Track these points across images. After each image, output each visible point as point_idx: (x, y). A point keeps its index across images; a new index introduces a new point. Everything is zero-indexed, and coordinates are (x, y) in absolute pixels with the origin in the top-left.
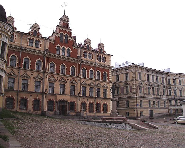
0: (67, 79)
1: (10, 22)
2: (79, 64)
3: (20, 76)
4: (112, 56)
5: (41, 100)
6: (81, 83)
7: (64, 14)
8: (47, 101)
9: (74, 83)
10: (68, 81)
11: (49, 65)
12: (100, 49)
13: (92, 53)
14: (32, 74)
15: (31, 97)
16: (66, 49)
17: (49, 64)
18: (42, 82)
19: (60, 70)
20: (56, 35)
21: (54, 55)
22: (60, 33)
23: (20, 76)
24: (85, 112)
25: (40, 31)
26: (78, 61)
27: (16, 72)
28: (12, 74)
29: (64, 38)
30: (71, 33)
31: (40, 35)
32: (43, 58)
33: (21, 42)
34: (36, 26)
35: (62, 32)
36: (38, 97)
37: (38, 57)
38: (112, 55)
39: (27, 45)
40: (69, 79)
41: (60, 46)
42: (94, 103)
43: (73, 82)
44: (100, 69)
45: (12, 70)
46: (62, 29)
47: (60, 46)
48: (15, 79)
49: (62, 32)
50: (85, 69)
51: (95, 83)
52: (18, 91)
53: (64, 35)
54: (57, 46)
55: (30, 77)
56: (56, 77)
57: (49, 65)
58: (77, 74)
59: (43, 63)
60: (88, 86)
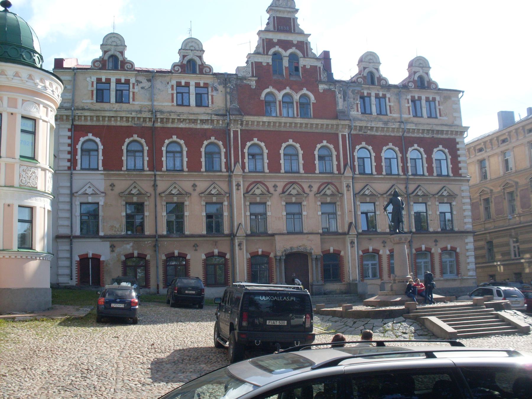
0: (305, 186)
1: (113, 48)
2: (344, 136)
4: (463, 92)
5: (228, 256)
6: (357, 191)
8: (249, 256)
9: (333, 195)
10: (311, 191)
11: (246, 150)
12: (416, 78)
13: (388, 95)
14: (194, 186)
15: (196, 250)
18: (226, 203)
19: (282, 161)
20: (260, 60)
23: (159, 194)
25: (207, 59)
27: (146, 186)
28: (133, 192)
29: (286, 63)
30: (307, 44)
31: (208, 70)
33: (151, 99)
35: (277, 48)
36: (217, 248)
37: (205, 134)
38: (460, 92)
40: (312, 185)
41: (275, 92)
43: (329, 192)
44: (421, 142)
45: (135, 182)
48: (145, 204)
49: (277, 48)
51: (406, 188)
52: (156, 237)
55: (188, 194)
56: (270, 185)
57: (243, 154)
58: (338, 166)
59: (225, 146)
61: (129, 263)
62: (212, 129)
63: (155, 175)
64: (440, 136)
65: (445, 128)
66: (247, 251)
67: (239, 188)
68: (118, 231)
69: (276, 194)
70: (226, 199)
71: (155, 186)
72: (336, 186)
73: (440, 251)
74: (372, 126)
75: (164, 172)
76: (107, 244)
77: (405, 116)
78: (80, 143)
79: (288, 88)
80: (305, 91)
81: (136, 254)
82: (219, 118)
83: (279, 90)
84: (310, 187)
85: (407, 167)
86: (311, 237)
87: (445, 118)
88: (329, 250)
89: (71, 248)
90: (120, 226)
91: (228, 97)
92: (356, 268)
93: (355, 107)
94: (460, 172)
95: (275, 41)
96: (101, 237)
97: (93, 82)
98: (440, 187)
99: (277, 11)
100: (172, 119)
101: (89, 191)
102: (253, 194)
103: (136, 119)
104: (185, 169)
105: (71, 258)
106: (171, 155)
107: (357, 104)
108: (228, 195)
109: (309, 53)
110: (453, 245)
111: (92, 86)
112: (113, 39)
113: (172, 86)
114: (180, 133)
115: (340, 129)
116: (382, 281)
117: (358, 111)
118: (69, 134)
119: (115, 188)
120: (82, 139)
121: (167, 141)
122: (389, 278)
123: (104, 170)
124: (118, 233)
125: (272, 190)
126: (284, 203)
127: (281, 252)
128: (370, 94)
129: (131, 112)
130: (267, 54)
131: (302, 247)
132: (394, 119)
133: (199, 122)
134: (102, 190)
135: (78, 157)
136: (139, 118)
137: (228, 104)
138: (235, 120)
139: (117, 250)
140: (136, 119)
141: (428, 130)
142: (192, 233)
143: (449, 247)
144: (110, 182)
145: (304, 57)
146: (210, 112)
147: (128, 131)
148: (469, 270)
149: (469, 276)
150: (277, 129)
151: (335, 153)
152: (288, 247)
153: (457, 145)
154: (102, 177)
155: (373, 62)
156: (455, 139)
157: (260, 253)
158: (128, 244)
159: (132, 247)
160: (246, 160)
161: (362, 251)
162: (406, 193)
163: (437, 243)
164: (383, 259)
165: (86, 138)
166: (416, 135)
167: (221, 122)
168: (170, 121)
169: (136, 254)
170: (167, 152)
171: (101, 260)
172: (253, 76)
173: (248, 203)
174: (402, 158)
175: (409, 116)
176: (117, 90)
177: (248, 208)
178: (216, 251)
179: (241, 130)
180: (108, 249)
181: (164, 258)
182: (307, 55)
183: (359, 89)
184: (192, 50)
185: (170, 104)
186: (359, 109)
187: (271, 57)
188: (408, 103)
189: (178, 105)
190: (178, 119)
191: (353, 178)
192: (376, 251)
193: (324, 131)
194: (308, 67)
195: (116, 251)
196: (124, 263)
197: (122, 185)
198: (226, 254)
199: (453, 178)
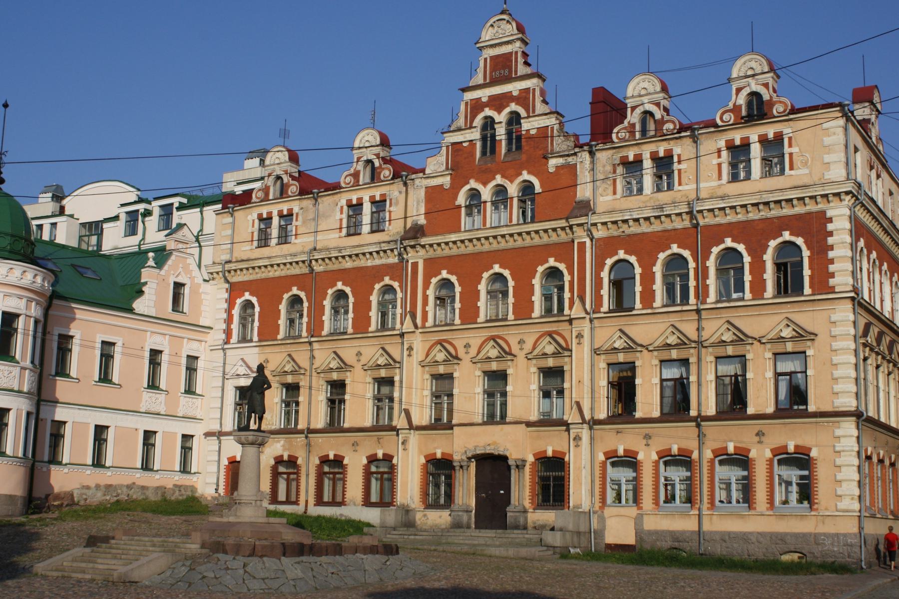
3: (314, 370)
9: (556, 354)
10: (521, 349)
13: (677, 151)
14: (359, 354)
15: (355, 451)
16: (513, 189)
17: (426, 286)
18: (397, 378)
21: (453, 237)
24: (633, 511)
26: (571, 227)
29: (501, 132)
34: (366, 138)
35: (488, 112)
37: (377, 273)
39: (337, 235)
41: (479, 187)
42: (695, 455)
43: (550, 349)
46: (484, 94)
47: (479, 187)
49: (488, 112)
50: (628, 261)
51: (698, 329)
53: (501, 118)
54: (467, 187)
56: (459, 345)
59: (402, 291)
60: (645, 351)
63: (310, 343)
64: (787, 211)
66: (420, 452)
67: (412, 352)
68: (269, 424)
71: (313, 357)
73: (768, 454)
74: (635, 217)
75: (325, 336)
79: (498, 177)
83: (485, 184)
84: (521, 342)
85: (706, 287)
90: (272, 417)
92: (581, 484)
94: (832, 282)
95: (484, 100)
97: (253, 221)
104: (350, 330)
110: (800, 443)
111: (253, 226)
113: (342, 207)
118: (226, 295)
120: (239, 301)
121: (330, 292)
122: (654, 506)
123: (260, 341)
124: (269, 427)
127: (460, 454)
129: (285, 256)
130: (471, 127)
131: (492, 447)
135: (235, 326)
141: (753, 205)
145: (529, 117)
146: (387, 239)
147: (286, 282)
151: (567, 278)
152: (471, 446)
153: (829, 225)
156: (823, 213)
158: (279, 442)
159: (283, 446)
160: (430, 308)
163: (763, 439)
164: (756, 470)
165: (243, 299)
172: (447, 169)
174: (696, 270)
179: (426, 261)
181: (317, 462)
182: (534, 111)
184: (366, 147)
185: (337, 235)
187: (479, 129)
188: (719, 156)
189: (349, 235)
191: (591, 321)
194: (533, 132)
195: (265, 452)
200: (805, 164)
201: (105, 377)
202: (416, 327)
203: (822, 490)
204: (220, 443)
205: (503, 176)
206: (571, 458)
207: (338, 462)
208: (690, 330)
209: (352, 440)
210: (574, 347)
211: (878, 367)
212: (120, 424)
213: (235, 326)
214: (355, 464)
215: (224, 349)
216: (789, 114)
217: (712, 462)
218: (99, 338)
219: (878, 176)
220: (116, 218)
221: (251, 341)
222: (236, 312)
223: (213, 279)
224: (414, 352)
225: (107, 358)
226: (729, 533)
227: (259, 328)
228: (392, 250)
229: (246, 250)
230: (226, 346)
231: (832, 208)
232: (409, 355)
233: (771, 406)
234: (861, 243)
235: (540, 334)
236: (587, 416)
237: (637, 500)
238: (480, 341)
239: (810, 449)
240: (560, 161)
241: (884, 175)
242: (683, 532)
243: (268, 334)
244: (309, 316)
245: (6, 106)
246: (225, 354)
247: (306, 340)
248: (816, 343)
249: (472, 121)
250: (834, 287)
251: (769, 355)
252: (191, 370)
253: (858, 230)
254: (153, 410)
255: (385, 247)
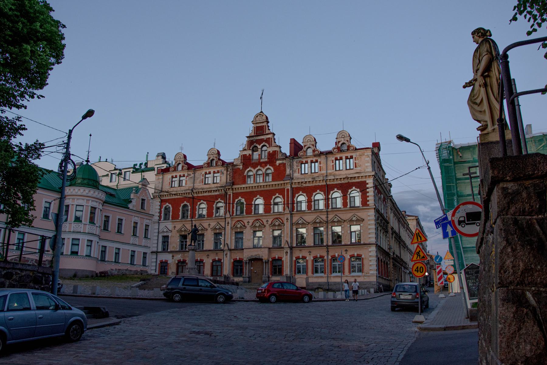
0: (264, 221)
2: (288, 190)
5: (222, 261)
7: (262, 112)
8: (232, 261)
9: (279, 225)
10: (267, 223)
13: (319, 160)
17: (234, 201)
18: (223, 233)
22: (251, 149)
24: (305, 276)
32: (224, 197)
39: (202, 184)
42: (325, 258)
45: (184, 225)
53: (259, 147)
54: (248, 169)
56: (246, 222)
61: (180, 264)
62: (219, 195)
63: (192, 221)
65: (357, 175)
69: (248, 227)
70: (223, 230)
72: (282, 220)
76: (171, 255)
77: (329, 171)
78: (163, 208)
80: (268, 166)
81: (182, 260)
82: (221, 188)
83: (254, 168)
84: (267, 221)
86: (263, 249)
87: (359, 168)
88: (275, 257)
89: (157, 257)
91: (228, 176)
92: (288, 268)
93: (297, 171)
94: (368, 203)
96: (168, 252)
98: (351, 214)
99: (257, 123)
100: (201, 192)
101: (165, 230)
102: (236, 227)
103: (185, 194)
105: (156, 262)
106: (201, 209)
107: (299, 169)
108: (223, 229)
109: (273, 143)
110: (359, 253)
112: (179, 156)
113: (203, 175)
114: (205, 198)
115: (286, 186)
116: (307, 276)
117: (299, 173)
118: (159, 204)
119: (176, 228)
120: (164, 206)
121: (199, 203)
123: (172, 219)
125: (246, 224)
126: (252, 231)
128: (307, 161)
130: (250, 150)
132: (323, 174)
133: (213, 191)
134: (170, 229)
135: (162, 215)
136: (186, 193)
137: (228, 180)
138: (229, 189)
139: (174, 258)
140: (185, 194)
142: (206, 249)
143: (356, 255)
144: (173, 226)
145: (270, 147)
147: (182, 200)
148: (371, 270)
149: (371, 274)
150: (251, 190)
152: (250, 256)
154: (171, 223)
155: (310, 141)
156: (366, 181)
157: (238, 259)
158: (179, 255)
161: (296, 258)
162: (326, 221)
166: (336, 182)
167: (223, 190)
168: (200, 192)
169: (182, 260)
170: (199, 208)
171: (169, 262)
172: (241, 163)
173: (234, 232)
175: (333, 171)
176: (180, 181)
177: (234, 235)
178: (217, 258)
179: (233, 193)
180: (171, 258)
182: (271, 145)
183: (300, 159)
185: (202, 184)
186: (300, 172)
188: (333, 163)
189: (205, 184)
190: (204, 191)
191: (291, 214)
192: (304, 258)
193: (277, 188)
196: (177, 264)
197: (179, 226)
198: (221, 260)
199: (361, 208)
200: (360, 166)
201: (119, 231)
202: (230, 216)
203: (366, 268)
204: (157, 255)
205: (261, 166)
206: (284, 259)
207: (202, 261)
208: (324, 217)
209: (207, 254)
210: (285, 223)
211: (381, 230)
212: (123, 248)
213: (162, 215)
214: (208, 262)
215: (159, 223)
216: (355, 150)
217: (331, 260)
218: (118, 217)
219: (380, 171)
220: (107, 175)
221: (169, 219)
222: (163, 210)
223: (155, 198)
224: (230, 224)
225: (120, 224)
226: (335, 282)
227: (172, 215)
228: (221, 190)
229: (166, 187)
230: (160, 222)
231: (368, 180)
232: (228, 225)
233: (349, 242)
234: (376, 191)
235: (273, 219)
236: (290, 246)
237: (306, 273)
238: (252, 221)
239: (362, 255)
240: (281, 162)
241: (381, 170)
242: (322, 282)
243: (175, 217)
244: (190, 212)
245: (91, 135)
246: (159, 224)
247: (190, 220)
248: (363, 222)
249: (250, 148)
250: (369, 205)
251: (349, 226)
252: (146, 230)
253: (376, 187)
254: (134, 243)
255: (219, 188)
